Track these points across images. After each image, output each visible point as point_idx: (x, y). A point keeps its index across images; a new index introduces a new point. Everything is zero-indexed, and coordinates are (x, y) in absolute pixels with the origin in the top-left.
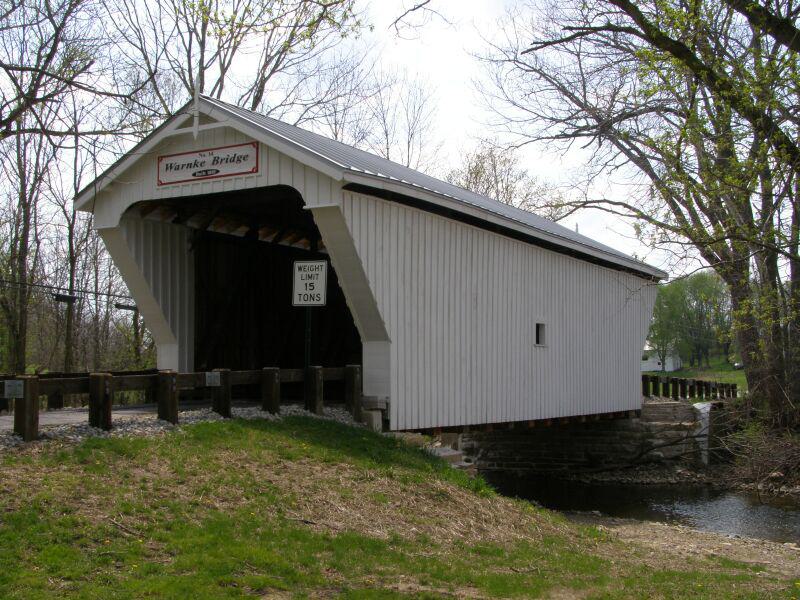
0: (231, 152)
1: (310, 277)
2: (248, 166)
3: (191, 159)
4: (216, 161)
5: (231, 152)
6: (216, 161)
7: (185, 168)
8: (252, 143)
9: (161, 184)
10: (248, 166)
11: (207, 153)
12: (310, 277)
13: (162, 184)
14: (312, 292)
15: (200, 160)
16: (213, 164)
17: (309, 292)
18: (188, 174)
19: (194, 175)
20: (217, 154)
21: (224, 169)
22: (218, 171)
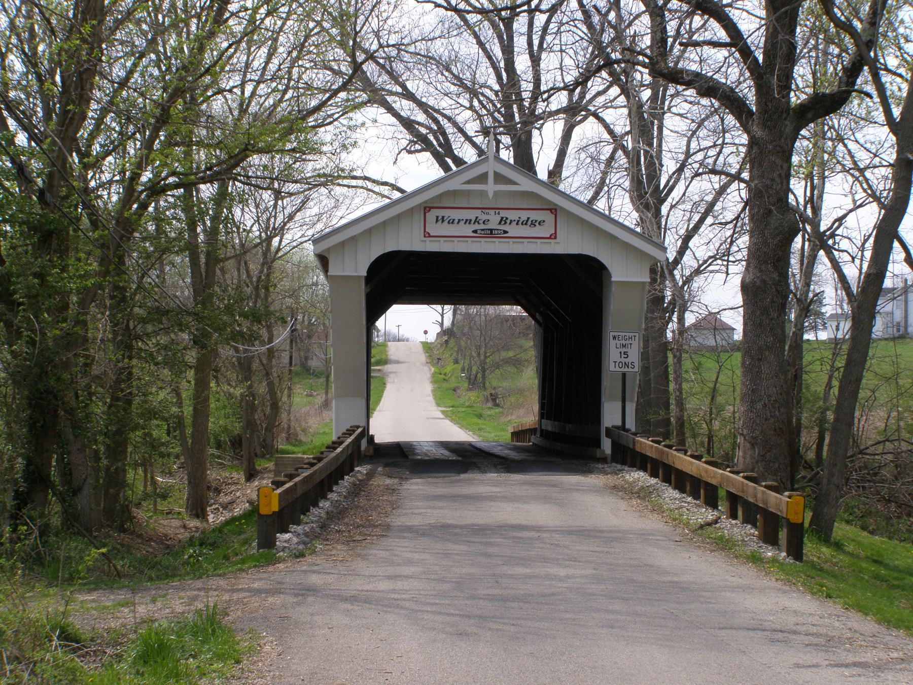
0: (524, 215)
1: (624, 346)
2: (546, 231)
3: (472, 215)
4: (503, 221)
5: (524, 215)
6: (503, 221)
7: (462, 223)
8: (550, 210)
9: (427, 235)
10: (546, 231)
11: (492, 212)
12: (624, 346)
13: (430, 236)
14: (627, 360)
15: (483, 217)
16: (500, 223)
17: (623, 360)
18: (468, 230)
19: (475, 232)
20: (504, 214)
21: (513, 230)
22: (505, 232)
